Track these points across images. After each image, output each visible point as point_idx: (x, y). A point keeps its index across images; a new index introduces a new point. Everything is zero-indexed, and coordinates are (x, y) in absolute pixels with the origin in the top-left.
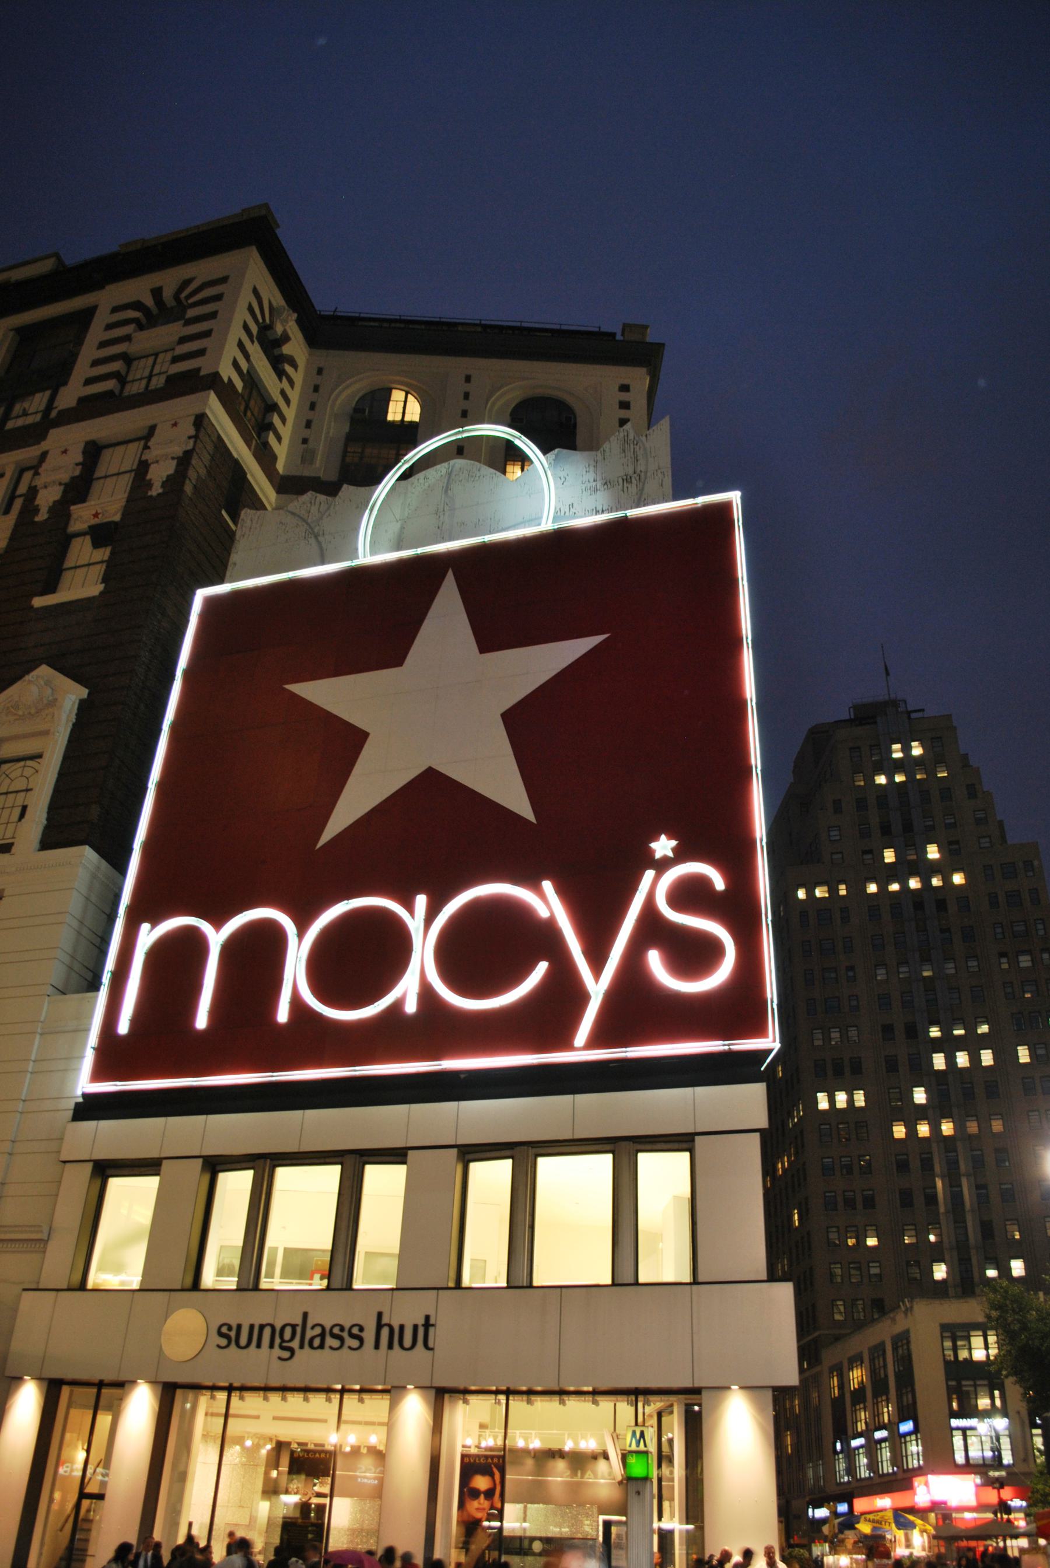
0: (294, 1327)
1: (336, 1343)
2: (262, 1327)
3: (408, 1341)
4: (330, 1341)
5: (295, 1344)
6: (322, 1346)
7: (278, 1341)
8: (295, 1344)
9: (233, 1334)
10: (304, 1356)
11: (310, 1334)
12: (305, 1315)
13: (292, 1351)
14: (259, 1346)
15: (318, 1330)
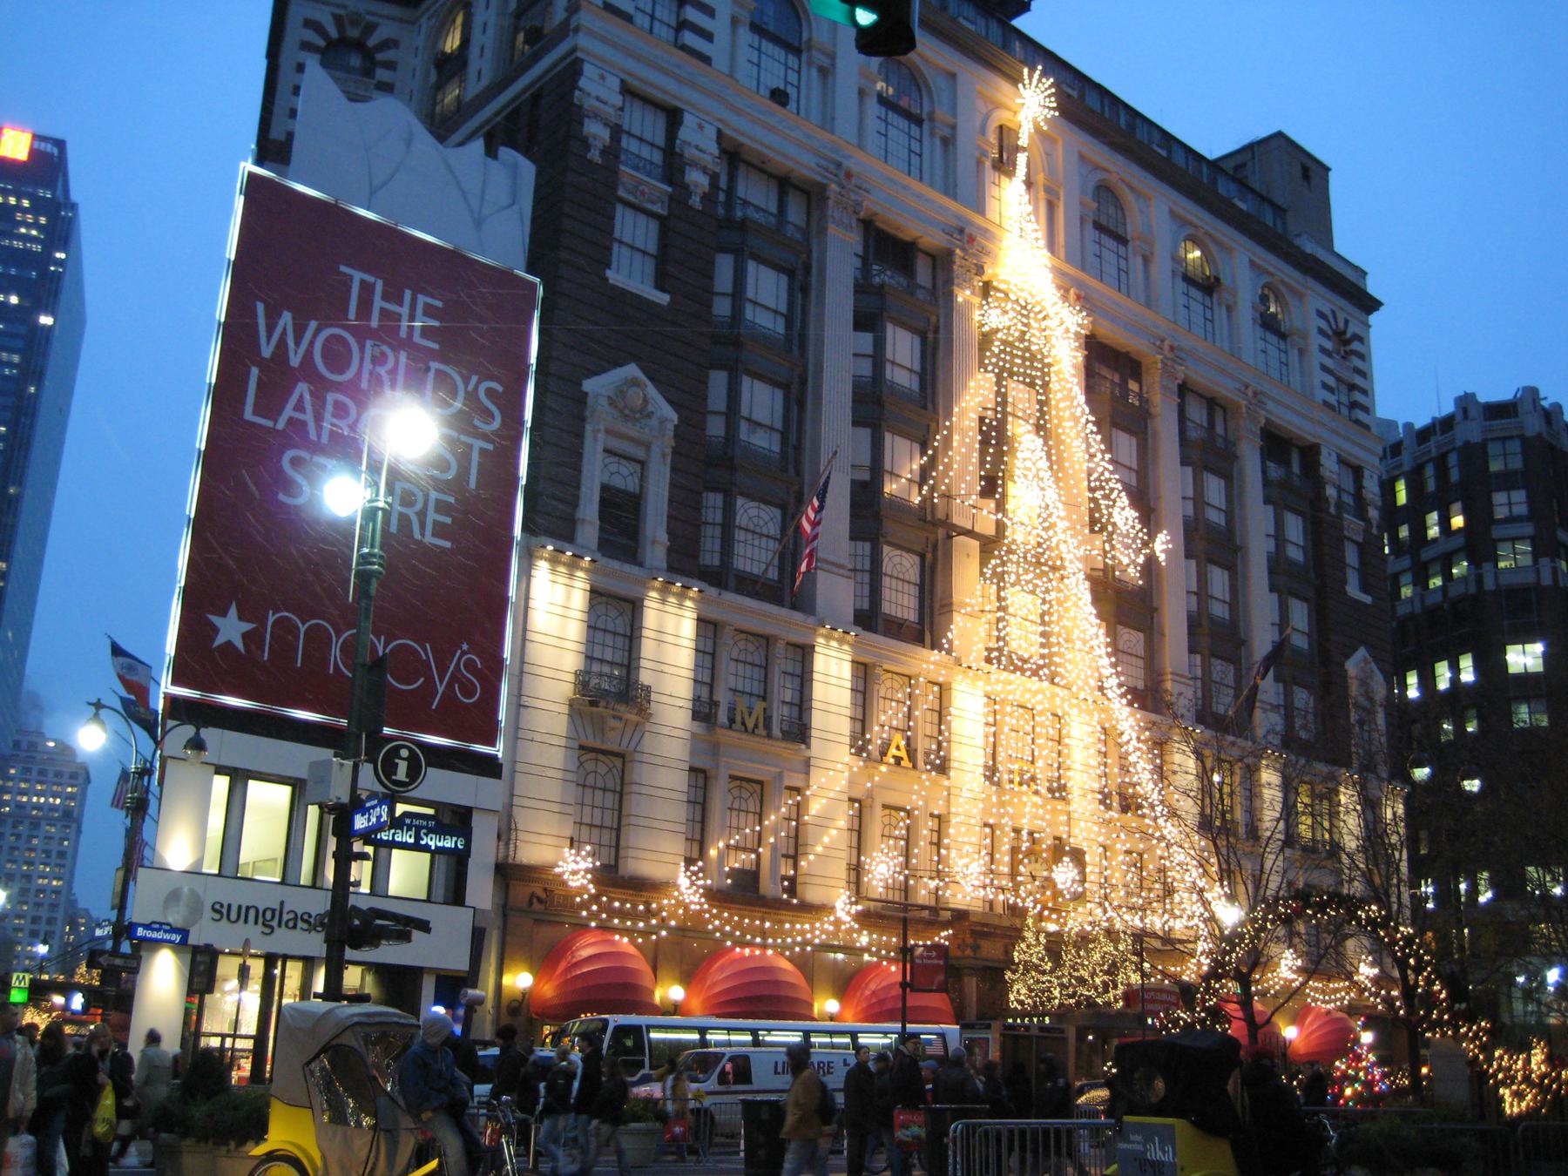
0: (273, 911)
1: (305, 926)
2: (248, 908)
3: (233, 916)
4: (300, 924)
5: (275, 923)
6: (295, 927)
7: (261, 920)
8: (275, 923)
9: (225, 911)
10: (281, 933)
11: (286, 917)
12: (282, 903)
13: (272, 928)
14: (246, 921)
15: (292, 916)
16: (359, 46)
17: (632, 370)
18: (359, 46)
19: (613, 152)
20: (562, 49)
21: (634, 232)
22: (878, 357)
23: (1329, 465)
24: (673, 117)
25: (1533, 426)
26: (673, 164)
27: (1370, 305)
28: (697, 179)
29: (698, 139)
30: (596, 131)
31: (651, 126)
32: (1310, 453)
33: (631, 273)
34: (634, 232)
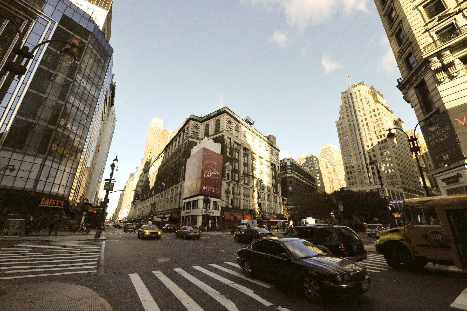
16: (196, 127)
17: (228, 163)
18: (196, 127)
19: (227, 143)
20: (222, 133)
21: (228, 150)
22: (244, 160)
23: (276, 166)
24: (230, 139)
25: (291, 161)
26: (230, 144)
27: (279, 151)
28: (232, 145)
29: (232, 141)
30: (225, 141)
31: (229, 140)
32: (275, 165)
33: (228, 154)
34: (228, 150)
